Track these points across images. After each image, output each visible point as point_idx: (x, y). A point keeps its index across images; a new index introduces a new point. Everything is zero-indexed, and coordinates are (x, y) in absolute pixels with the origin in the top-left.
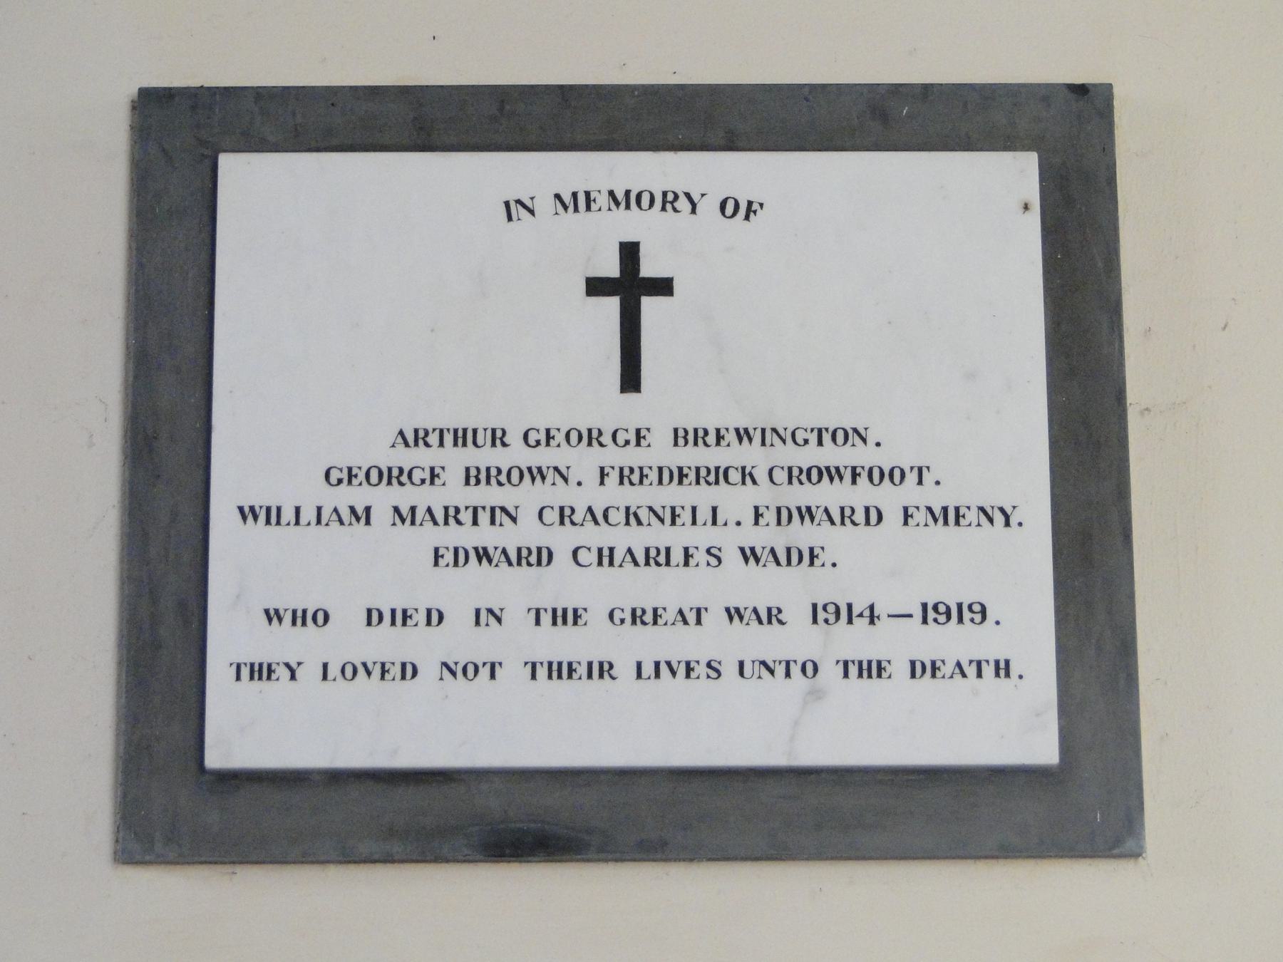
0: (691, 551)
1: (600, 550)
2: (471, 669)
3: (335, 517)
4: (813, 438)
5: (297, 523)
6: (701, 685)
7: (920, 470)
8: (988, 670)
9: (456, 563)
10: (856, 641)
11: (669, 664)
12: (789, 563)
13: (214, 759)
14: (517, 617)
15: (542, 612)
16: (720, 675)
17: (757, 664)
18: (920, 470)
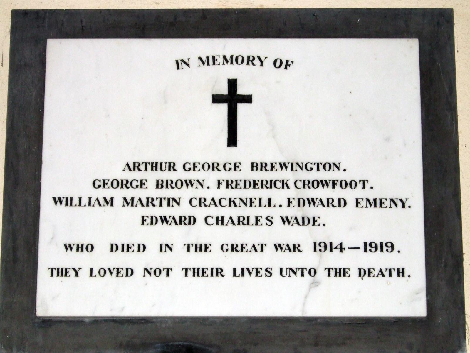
0: (259, 218)
1: (217, 218)
2: (158, 271)
3: (97, 202)
4: (315, 167)
5: (80, 205)
6: (263, 280)
7: (364, 182)
8: (394, 273)
9: (152, 224)
10: (335, 260)
11: (248, 269)
12: (303, 224)
13: (40, 312)
14: (179, 248)
15: (191, 246)
16: (271, 275)
17: (288, 270)
18: (364, 182)
